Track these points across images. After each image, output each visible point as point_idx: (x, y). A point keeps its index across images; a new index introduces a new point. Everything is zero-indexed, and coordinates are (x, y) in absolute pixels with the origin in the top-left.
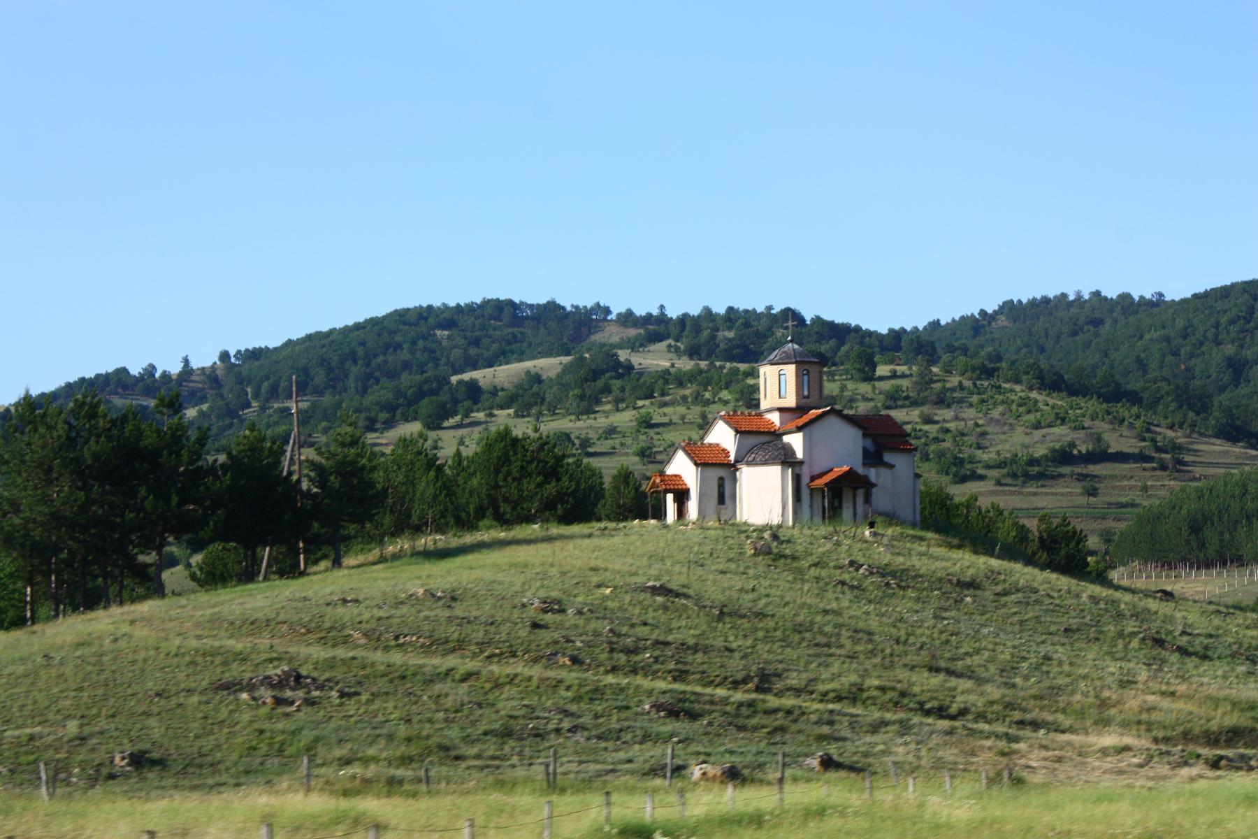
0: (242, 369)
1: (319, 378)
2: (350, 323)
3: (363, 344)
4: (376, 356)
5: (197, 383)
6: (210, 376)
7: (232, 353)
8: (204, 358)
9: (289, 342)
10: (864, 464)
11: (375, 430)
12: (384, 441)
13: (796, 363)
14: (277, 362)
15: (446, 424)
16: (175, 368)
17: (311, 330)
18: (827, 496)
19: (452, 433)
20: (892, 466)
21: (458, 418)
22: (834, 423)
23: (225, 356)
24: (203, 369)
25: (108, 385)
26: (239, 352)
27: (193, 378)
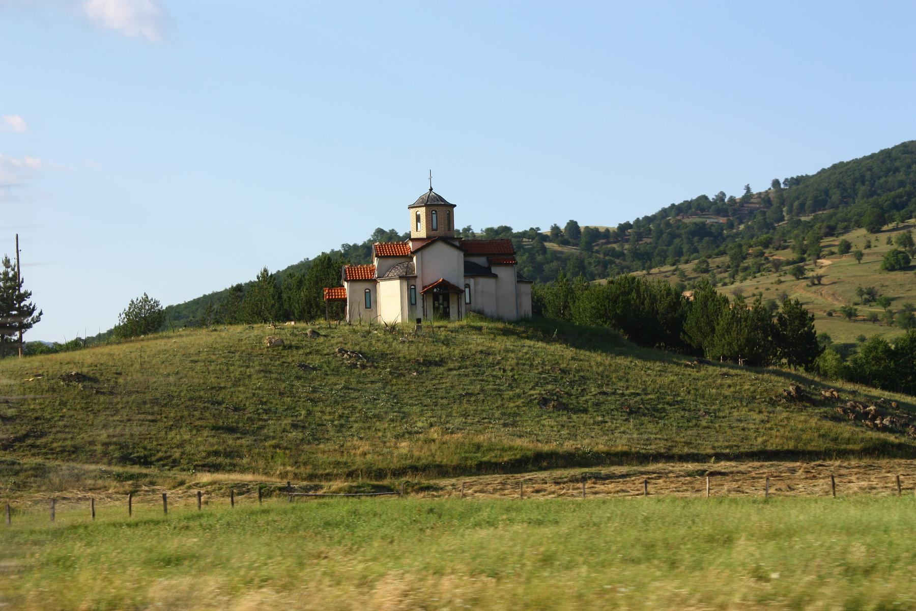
0: (784, 193)
1: (836, 196)
2: (868, 154)
3: (870, 169)
4: (879, 178)
5: (755, 204)
6: (765, 198)
7: (781, 181)
8: (761, 186)
9: (823, 170)
10: (465, 276)
11: (832, 235)
12: (837, 243)
13: (426, 205)
14: (807, 186)
15: (885, 228)
16: (739, 194)
17: (837, 162)
18: (437, 298)
19: (888, 234)
20: (495, 276)
21: (894, 224)
22: (441, 247)
23: (776, 183)
24: (760, 193)
25: (690, 208)
26: (786, 180)
27: (752, 200)
